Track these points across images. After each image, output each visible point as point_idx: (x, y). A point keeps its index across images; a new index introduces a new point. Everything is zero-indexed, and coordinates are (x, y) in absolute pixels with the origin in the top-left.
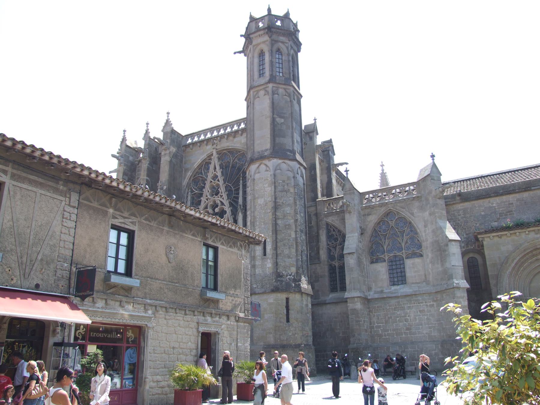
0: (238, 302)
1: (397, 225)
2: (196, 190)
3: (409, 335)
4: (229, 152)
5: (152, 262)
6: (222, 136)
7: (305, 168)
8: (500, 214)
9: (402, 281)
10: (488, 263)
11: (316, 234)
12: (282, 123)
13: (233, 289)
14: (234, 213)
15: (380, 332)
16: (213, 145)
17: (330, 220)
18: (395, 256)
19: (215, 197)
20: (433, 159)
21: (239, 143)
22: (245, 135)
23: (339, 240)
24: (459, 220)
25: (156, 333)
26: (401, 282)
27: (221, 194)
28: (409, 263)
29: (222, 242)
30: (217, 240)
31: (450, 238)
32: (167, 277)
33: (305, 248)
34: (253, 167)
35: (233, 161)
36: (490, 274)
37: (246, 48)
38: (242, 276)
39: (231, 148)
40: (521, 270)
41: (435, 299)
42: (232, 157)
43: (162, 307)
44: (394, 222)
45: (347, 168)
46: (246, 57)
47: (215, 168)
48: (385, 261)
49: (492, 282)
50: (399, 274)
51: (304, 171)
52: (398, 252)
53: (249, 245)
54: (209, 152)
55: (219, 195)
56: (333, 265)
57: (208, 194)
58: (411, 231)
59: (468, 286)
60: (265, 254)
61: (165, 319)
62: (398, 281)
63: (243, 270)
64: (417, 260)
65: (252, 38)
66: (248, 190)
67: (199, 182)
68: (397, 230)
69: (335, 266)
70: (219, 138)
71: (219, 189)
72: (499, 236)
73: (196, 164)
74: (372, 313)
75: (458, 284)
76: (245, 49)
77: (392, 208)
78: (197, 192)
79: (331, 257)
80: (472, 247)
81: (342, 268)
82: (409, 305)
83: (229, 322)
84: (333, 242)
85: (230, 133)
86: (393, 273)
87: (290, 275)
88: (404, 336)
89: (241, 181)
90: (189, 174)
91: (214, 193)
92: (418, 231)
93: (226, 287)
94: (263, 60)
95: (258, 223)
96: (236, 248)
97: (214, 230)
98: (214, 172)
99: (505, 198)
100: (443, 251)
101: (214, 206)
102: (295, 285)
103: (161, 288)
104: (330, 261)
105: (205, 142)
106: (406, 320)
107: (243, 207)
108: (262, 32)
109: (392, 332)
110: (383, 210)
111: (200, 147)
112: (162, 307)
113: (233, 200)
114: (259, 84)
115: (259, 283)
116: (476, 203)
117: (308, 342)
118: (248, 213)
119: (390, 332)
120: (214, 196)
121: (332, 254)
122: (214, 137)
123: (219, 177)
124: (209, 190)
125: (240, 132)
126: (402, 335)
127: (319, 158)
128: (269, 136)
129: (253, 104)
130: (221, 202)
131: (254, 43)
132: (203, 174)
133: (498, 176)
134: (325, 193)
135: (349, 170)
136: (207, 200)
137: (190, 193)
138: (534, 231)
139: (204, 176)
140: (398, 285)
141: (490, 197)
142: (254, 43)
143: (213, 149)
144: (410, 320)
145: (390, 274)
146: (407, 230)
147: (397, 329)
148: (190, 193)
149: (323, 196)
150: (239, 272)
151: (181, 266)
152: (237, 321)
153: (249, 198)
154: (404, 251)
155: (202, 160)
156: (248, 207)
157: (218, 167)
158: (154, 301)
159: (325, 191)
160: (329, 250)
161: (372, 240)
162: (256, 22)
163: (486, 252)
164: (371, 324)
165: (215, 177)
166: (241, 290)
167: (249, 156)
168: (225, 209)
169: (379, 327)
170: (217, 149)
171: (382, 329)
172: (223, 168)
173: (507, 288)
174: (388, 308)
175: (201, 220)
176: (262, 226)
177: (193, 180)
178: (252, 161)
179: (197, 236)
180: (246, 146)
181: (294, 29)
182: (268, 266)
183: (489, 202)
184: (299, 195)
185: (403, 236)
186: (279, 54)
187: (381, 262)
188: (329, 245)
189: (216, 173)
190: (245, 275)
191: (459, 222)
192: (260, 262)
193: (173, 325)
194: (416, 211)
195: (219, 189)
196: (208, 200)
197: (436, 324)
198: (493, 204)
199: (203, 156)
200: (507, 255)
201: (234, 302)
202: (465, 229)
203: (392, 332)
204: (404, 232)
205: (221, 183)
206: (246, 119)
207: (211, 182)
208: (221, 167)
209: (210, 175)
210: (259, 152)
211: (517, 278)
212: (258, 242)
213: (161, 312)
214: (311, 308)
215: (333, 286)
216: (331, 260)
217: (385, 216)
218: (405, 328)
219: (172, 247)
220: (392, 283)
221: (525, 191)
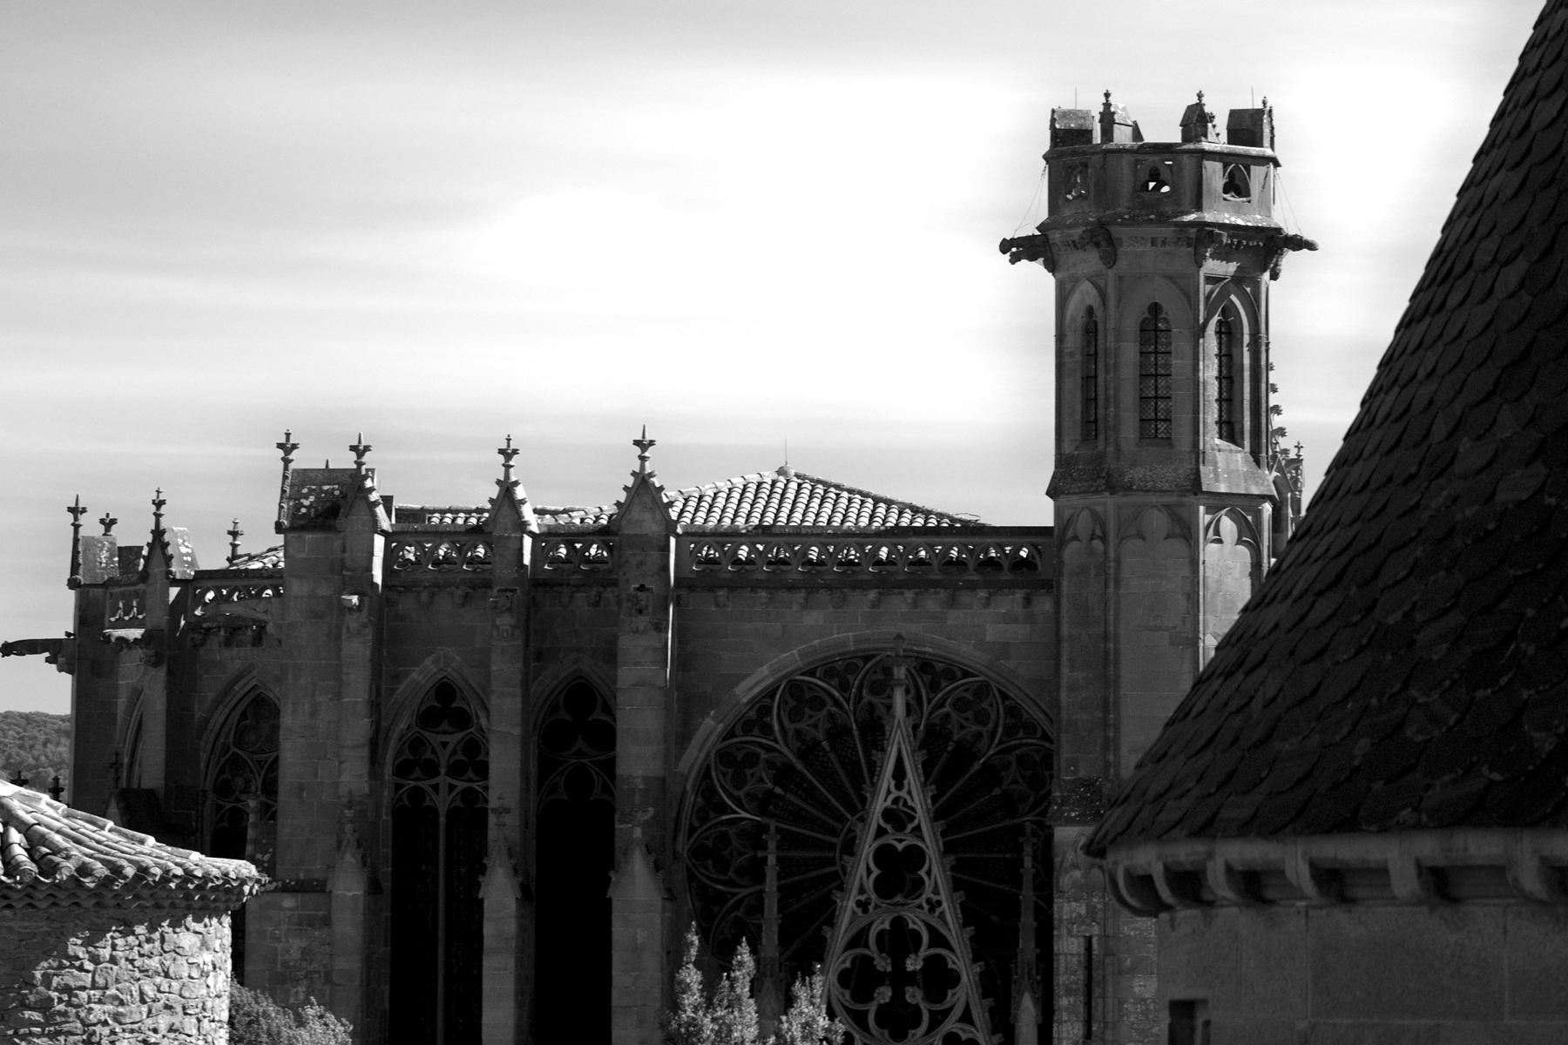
14: (998, 992)
27: (935, 898)
47: (899, 775)
57: (869, 884)
98: (895, 793)
129: (1118, 561)
130: (930, 928)
196: (865, 911)
205: (931, 845)
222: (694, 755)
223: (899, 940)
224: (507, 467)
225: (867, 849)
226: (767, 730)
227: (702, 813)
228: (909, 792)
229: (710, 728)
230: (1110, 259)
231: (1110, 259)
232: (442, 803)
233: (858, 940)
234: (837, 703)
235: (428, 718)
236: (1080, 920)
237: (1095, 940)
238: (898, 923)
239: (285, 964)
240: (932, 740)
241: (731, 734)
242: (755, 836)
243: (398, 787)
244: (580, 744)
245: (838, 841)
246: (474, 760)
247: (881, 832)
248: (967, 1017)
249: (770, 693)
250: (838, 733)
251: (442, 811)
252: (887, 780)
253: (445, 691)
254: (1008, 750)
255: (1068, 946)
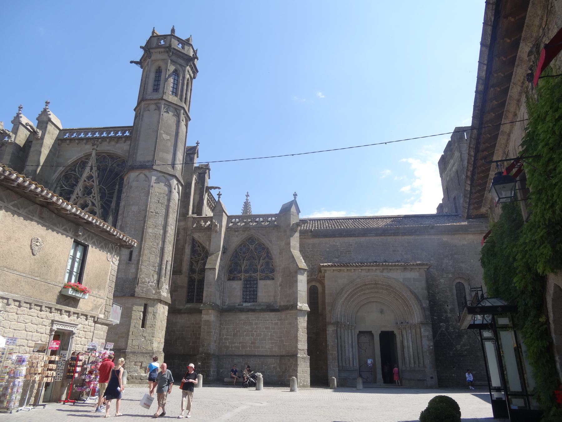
0: (100, 303)
1: (256, 249)
2: (66, 186)
3: (253, 349)
4: (108, 156)
5: (13, 252)
6: (104, 139)
7: (182, 185)
8: (341, 252)
9: (254, 299)
10: (327, 292)
11: (182, 247)
12: (167, 140)
13: (96, 289)
15: (228, 344)
16: (93, 146)
17: (196, 236)
18: (251, 277)
19: (86, 197)
20: (295, 198)
21: (121, 149)
22: (128, 143)
23: (202, 255)
24: (308, 253)
25: (2, 328)
26: (253, 300)
27: (94, 195)
28: (261, 284)
29: (94, 241)
30: (89, 239)
31: (300, 267)
32: (27, 269)
33: (171, 259)
34: (133, 175)
35: (111, 166)
36: (326, 301)
37: (144, 61)
38: (108, 278)
39: (111, 152)
40: (351, 301)
41: (280, 318)
42: (111, 161)
43: (15, 301)
44: (253, 247)
45: (220, 192)
46: (142, 69)
47: (91, 169)
48: (241, 280)
49: (328, 308)
50: (252, 293)
51: (180, 188)
52: (253, 272)
53: (120, 248)
54: (87, 152)
55: (91, 196)
56: (193, 278)
58: (268, 256)
59: (309, 310)
60: (130, 259)
61: (17, 314)
62: (250, 299)
63: (110, 271)
64: (269, 282)
65: (152, 53)
66: (123, 196)
67: (71, 178)
68: (255, 253)
69: (195, 279)
70: (100, 140)
71: (92, 190)
72: (338, 270)
73: (70, 160)
74: (223, 326)
75: (301, 307)
76: (142, 61)
77: (254, 234)
78: (66, 188)
79: (192, 270)
80: (315, 277)
81: (201, 282)
82: (256, 322)
83: (86, 322)
84: (197, 257)
85: (113, 138)
86: (247, 291)
87: (152, 282)
88: (248, 349)
89: (117, 186)
90: (61, 169)
91: (86, 193)
92: (273, 257)
93: (90, 286)
94: (159, 76)
95: (128, 229)
96: (106, 249)
97: (87, 229)
99: (347, 239)
100: (293, 277)
101: (83, 205)
102: (156, 292)
103: (18, 280)
104: (190, 273)
105: (85, 141)
106: (253, 335)
107: (115, 211)
108: (162, 50)
109: (238, 345)
110: (245, 235)
111: (77, 144)
112: (15, 301)
113: (105, 203)
114: (151, 98)
115: (120, 287)
116: (324, 240)
117: (159, 348)
118: (120, 217)
119: (236, 345)
120: (86, 195)
121: (194, 267)
122: (96, 138)
123: (94, 178)
124: (81, 189)
125: (123, 139)
126: (247, 348)
127: (195, 178)
129: (143, 115)
130: (92, 202)
131: (153, 58)
132: (77, 172)
133: (343, 220)
134: (195, 211)
135: (221, 194)
136: (77, 198)
137: (58, 188)
138: (365, 270)
139: (77, 174)
140: (250, 302)
141: (335, 237)
142: (153, 58)
143: (93, 149)
144: (256, 335)
145: (244, 291)
146: (264, 255)
147: (244, 342)
148: (58, 188)
149: (193, 213)
150: (106, 273)
151: (45, 260)
152: (95, 322)
153: (122, 204)
154: (258, 273)
155: (78, 158)
156: (120, 212)
157: (95, 169)
158: (7, 293)
159: (195, 210)
160: (191, 264)
161: (232, 259)
162: (159, 39)
163: (327, 283)
164: (220, 335)
166: (105, 291)
167: (130, 163)
168: (95, 210)
169: (227, 339)
170: (97, 151)
171: (230, 341)
172: (100, 171)
173: (339, 315)
174: (238, 322)
175: (76, 216)
176: (132, 232)
177: (64, 175)
178: (133, 168)
179: (69, 232)
180: (127, 154)
181: (193, 55)
182: (131, 271)
183: (334, 241)
184: (173, 209)
185: (260, 260)
186: (175, 75)
187: (238, 280)
188: (192, 259)
189: (92, 174)
190: (111, 277)
191: (308, 254)
192: (124, 266)
193: (25, 321)
194: (274, 239)
195: (92, 190)
197: (277, 340)
198: (336, 243)
199: (80, 154)
200: (342, 287)
201: (95, 303)
202: (312, 261)
203: (238, 345)
204: (261, 257)
205: (96, 184)
206: (132, 128)
207: (85, 181)
208: (98, 169)
209: (85, 175)
210: (140, 162)
211: (347, 307)
212: (129, 247)
213: (13, 306)
214: (167, 315)
215: (190, 297)
216: (192, 273)
217: (246, 240)
218: (250, 342)
219: (39, 239)
220: (244, 300)
221: (363, 236)
228: (93, 173)
247: (85, 181)
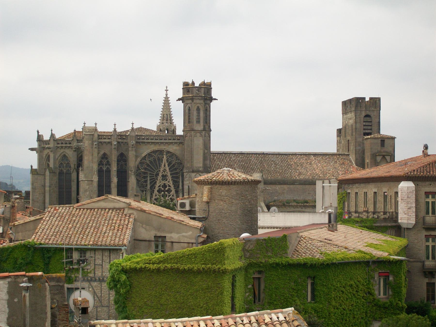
47: (165, 166)
57: (161, 179)
128: (202, 160)
165: (164, 171)
205: (169, 174)
209: (162, 170)
222: (137, 162)
223: (164, 186)
224: (115, 126)
225: (160, 174)
226: (146, 160)
227: (137, 170)
229: (139, 159)
230: (193, 101)
231: (193, 101)
232: (105, 169)
233: (159, 186)
234: (154, 156)
235: (102, 158)
236: (188, 184)
237: (190, 187)
238: (164, 184)
239: (86, 189)
240: (167, 161)
241: (141, 160)
242: (145, 173)
243: (99, 167)
244: (122, 161)
245: (155, 174)
246: (108, 164)
247: (162, 173)
248: (173, 196)
249: (146, 155)
250: (155, 160)
251: (104, 170)
252: (163, 166)
253: (105, 154)
254: (176, 163)
255: (186, 187)
